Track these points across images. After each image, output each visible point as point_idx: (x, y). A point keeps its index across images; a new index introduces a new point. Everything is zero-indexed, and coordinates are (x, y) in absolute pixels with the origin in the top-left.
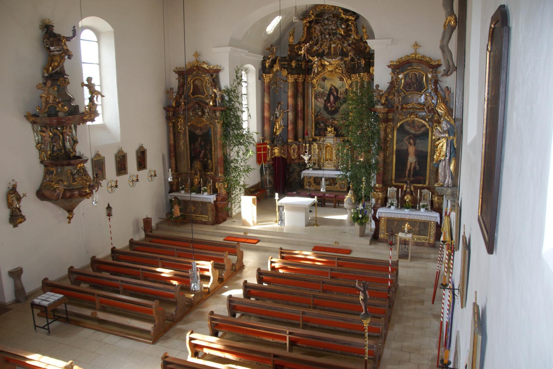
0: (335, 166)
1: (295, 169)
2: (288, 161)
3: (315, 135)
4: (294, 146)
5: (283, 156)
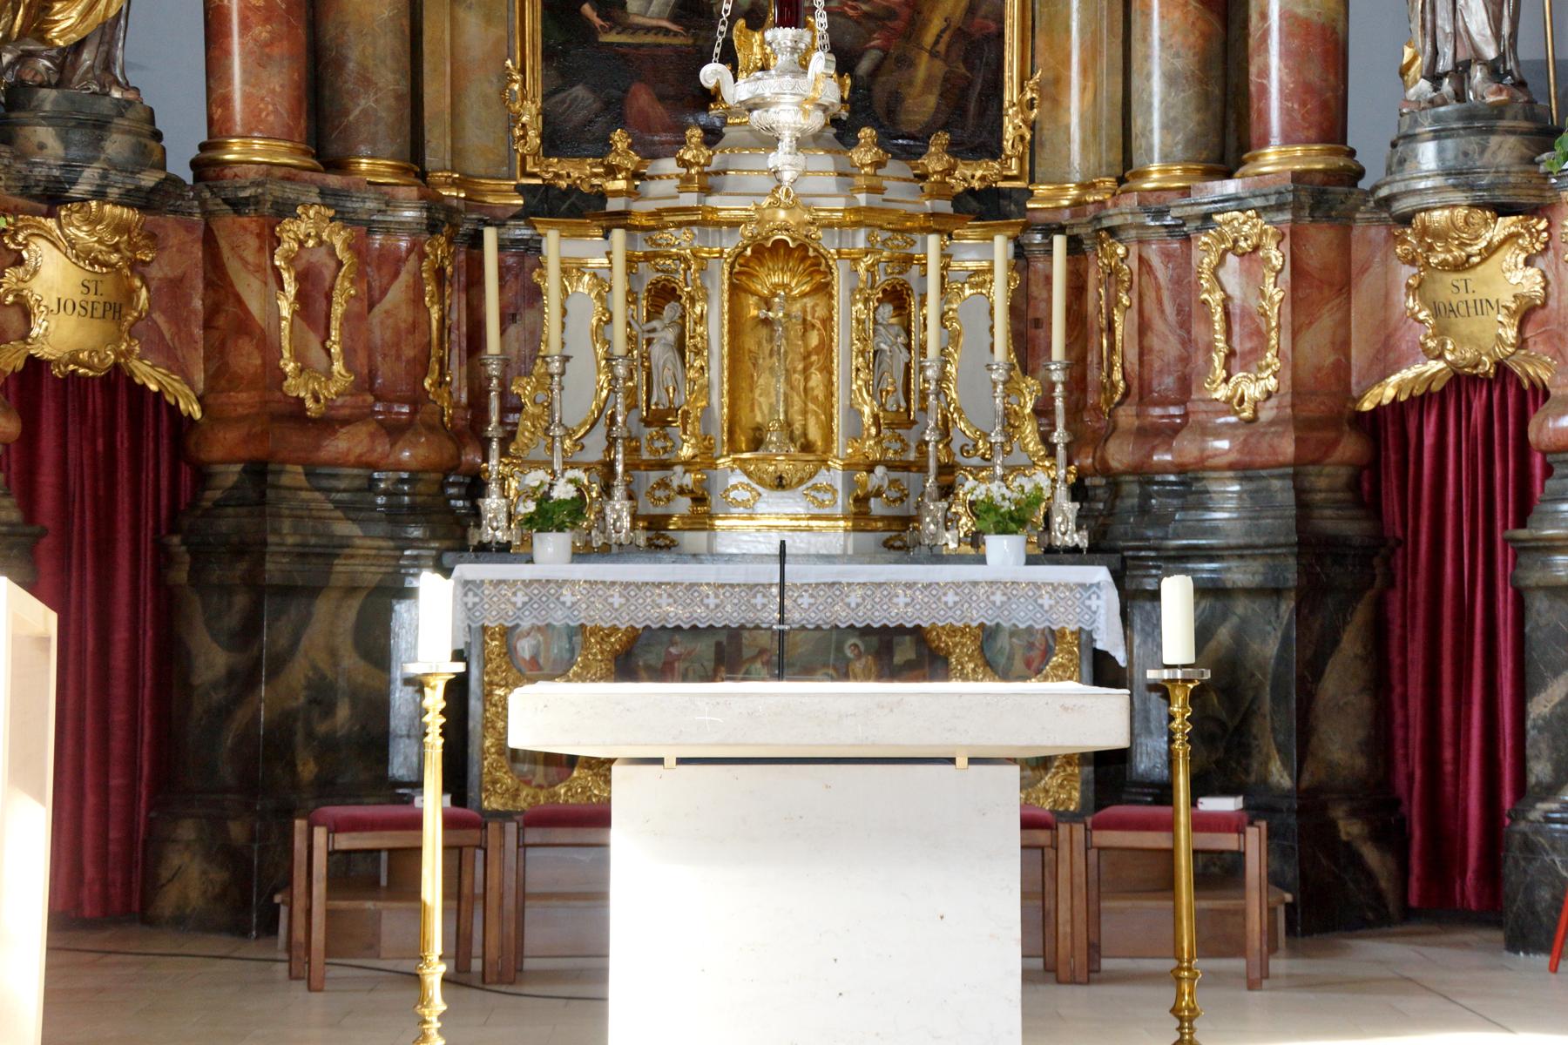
0: (860, 515)
1: (333, 550)
2: (226, 455)
3: (555, 141)
4: (308, 228)
5: (149, 375)
